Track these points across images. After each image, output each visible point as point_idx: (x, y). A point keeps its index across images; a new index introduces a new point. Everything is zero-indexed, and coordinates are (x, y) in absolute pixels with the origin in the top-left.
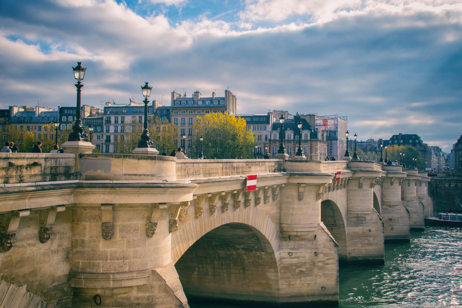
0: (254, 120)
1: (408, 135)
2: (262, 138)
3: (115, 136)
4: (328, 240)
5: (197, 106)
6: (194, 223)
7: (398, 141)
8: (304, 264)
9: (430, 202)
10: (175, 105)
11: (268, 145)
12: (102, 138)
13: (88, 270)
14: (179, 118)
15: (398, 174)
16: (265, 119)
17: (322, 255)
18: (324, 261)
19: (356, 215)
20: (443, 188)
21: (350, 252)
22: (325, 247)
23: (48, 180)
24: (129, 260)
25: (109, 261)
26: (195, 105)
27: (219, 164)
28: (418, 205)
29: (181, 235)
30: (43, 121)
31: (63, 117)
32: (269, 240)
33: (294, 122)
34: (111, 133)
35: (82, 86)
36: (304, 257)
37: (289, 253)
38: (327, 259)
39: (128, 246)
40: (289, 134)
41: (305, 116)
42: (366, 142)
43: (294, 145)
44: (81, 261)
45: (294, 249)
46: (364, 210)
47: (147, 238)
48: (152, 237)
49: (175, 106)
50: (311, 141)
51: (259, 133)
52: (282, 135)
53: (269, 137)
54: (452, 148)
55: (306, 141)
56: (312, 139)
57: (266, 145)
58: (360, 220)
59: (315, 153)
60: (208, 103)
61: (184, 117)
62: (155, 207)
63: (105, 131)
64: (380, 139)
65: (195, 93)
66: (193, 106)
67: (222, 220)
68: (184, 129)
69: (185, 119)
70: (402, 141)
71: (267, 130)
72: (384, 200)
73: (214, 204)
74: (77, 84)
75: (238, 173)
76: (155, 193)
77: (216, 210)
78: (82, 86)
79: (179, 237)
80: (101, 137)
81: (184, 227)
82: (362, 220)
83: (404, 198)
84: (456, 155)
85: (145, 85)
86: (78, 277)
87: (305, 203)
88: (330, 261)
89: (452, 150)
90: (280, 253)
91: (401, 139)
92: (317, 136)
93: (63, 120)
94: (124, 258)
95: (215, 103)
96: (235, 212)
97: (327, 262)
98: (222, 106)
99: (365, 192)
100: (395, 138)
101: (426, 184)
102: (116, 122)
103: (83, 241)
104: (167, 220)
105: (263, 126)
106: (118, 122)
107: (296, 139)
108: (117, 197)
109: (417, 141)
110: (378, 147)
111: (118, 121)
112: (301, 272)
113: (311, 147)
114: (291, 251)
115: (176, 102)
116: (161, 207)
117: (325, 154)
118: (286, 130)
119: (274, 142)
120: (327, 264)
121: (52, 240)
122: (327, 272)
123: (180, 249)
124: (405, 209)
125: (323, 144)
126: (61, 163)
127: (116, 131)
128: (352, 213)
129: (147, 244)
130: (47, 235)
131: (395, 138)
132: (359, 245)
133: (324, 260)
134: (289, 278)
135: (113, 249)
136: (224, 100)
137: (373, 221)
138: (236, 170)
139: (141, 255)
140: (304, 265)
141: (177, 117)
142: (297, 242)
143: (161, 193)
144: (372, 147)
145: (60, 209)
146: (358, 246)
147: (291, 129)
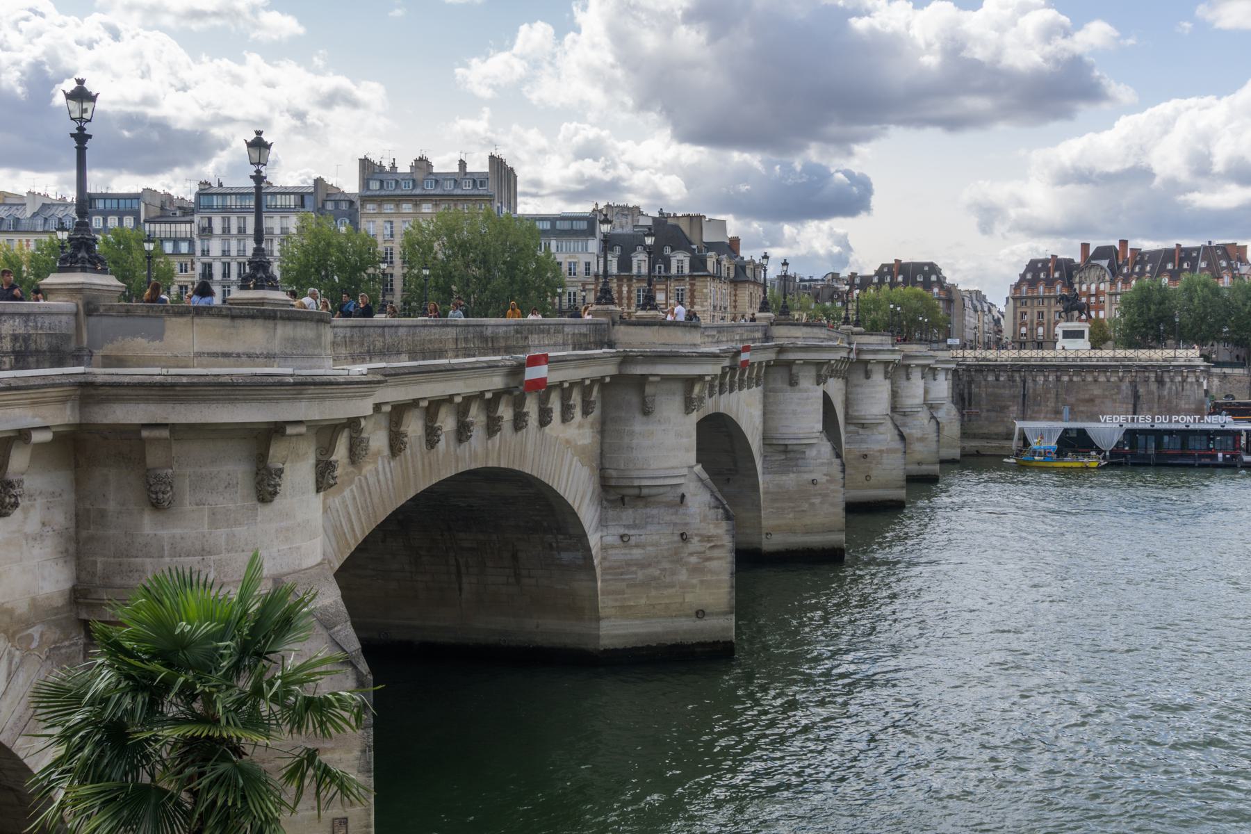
1: (913, 263)
2: (578, 270)
3: (224, 263)
4: (712, 504)
6: (387, 469)
7: (892, 279)
10: (368, 189)
11: (592, 287)
12: (193, 269)
13: (118, 581)
16: (583, 225)
18: (704, 552)
19: (782, 448)
20: (983, 383)
22: (704, 519)
23: (7, 366)
24: (217, 557)
25: (167, 559)
27: (449, 329)
28: (926, 422)
29: (354, 498)
30: (46, 229)
31: (94, 218)
32: (575, 508)
34: (215, 258)
35: (90, 137)
36: (655, 544)
37: (622, 537)
39: (214, 523)
42: (823, 280)
44: (100, 560)
45: (634, 526)
46: (801, 436)
47: (259, 505)
48: (271, 501)
49: (368, 193)
50: (692, 277)
51: (570, 257)
53: (593, 268)
54: (1008, 294)
55: (680, 278)
56: (695, 274)
57: (587, 287)
58: (791, 459)
59: (702, 306)
60: (449, 187)
62: (276, 432)
63: (198, 253)
65: (416, 161)
67: (457, 461)
68: (392, 249)
69: (394, 225)
70: (900, 278)
71: (590, 251)
72: (850, 412)
73: (436, 425)
74: (76, 132)
75: (496, 351)
76: (275, 399)
77: (442, 438)
78: (90, 137)
79: (349, 502)
80: (189, 266)
81: (362, 478)
82: (798, 459)
83: (896, 408)
84: (1015, 308)
85: (255, 136)
86: (95, 596)
88: (716, 553)
89: (1007, 298)
90: (601, 537)
91: (899, 274)
92: (706, 266)
93: (94, 225)
94: (204, 552)
95: (467, 189)
96: (489, 442)
97: (709, 554)
99: (805, 395)
100: (886, 270)
101: (947, 374)
102: (226, 230)
103: (103, 514)
104: (312, 461)
106: (229, 231)
108: (180, 408)
109: (934, 278)
111: (229, 227)
113: (692, 291)
114: (626, 532)
116: (290, 430)
117: (725, 308)
118: (635, 250)
121: (26, 511)
123: (353, 530)
124: (896, 432)
125: (720, 285)
126: (39, 325)
127: (225, 253)
128: (775, 442)
129: (259, 519)
130: (10, 497)
131: (886, 270)
133: (703, 549)
134: (623, 592)
135: (178, 531)
138: (490, 345)
139: (247, 544)
142: (640, 511)
143: (289, 399)
144: (834, 292)
145: (37, 437)
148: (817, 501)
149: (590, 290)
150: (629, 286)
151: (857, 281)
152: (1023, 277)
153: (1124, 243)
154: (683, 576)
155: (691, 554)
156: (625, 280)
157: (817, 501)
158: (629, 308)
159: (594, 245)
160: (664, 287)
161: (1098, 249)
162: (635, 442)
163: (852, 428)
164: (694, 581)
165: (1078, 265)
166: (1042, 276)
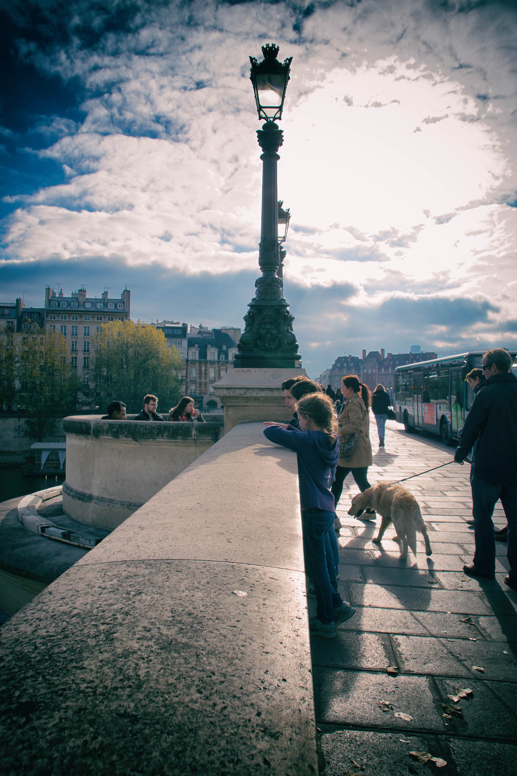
5: (84, 309)
14: (58, 326)
16: (180, 332)
26: (82, 309)
33: (214, 337)
40: (212, 354)
43: (219, 367)
49: (51, 309)
52: (203, 355)
60: (99, 306)
61: (65, 325)
65: (80, 290)
66: (79, 309)
69: (67, 328)
95: (111, 307)
98: (121, 311)
105: (178, 340)
107: (221, 359)
115: (52, 302)
119: (191, 363)
136: (124, 303)
147: (212, 346)
149: (184, 368)
150: (206, 367)
152: (334, 366)
153: (383, 350)
156: (203, 363)
158: (206, 379)
159: (185, 343)
160: (225, 368)
161: (370, 352)
165: (361, 360)
166: (345, 365)
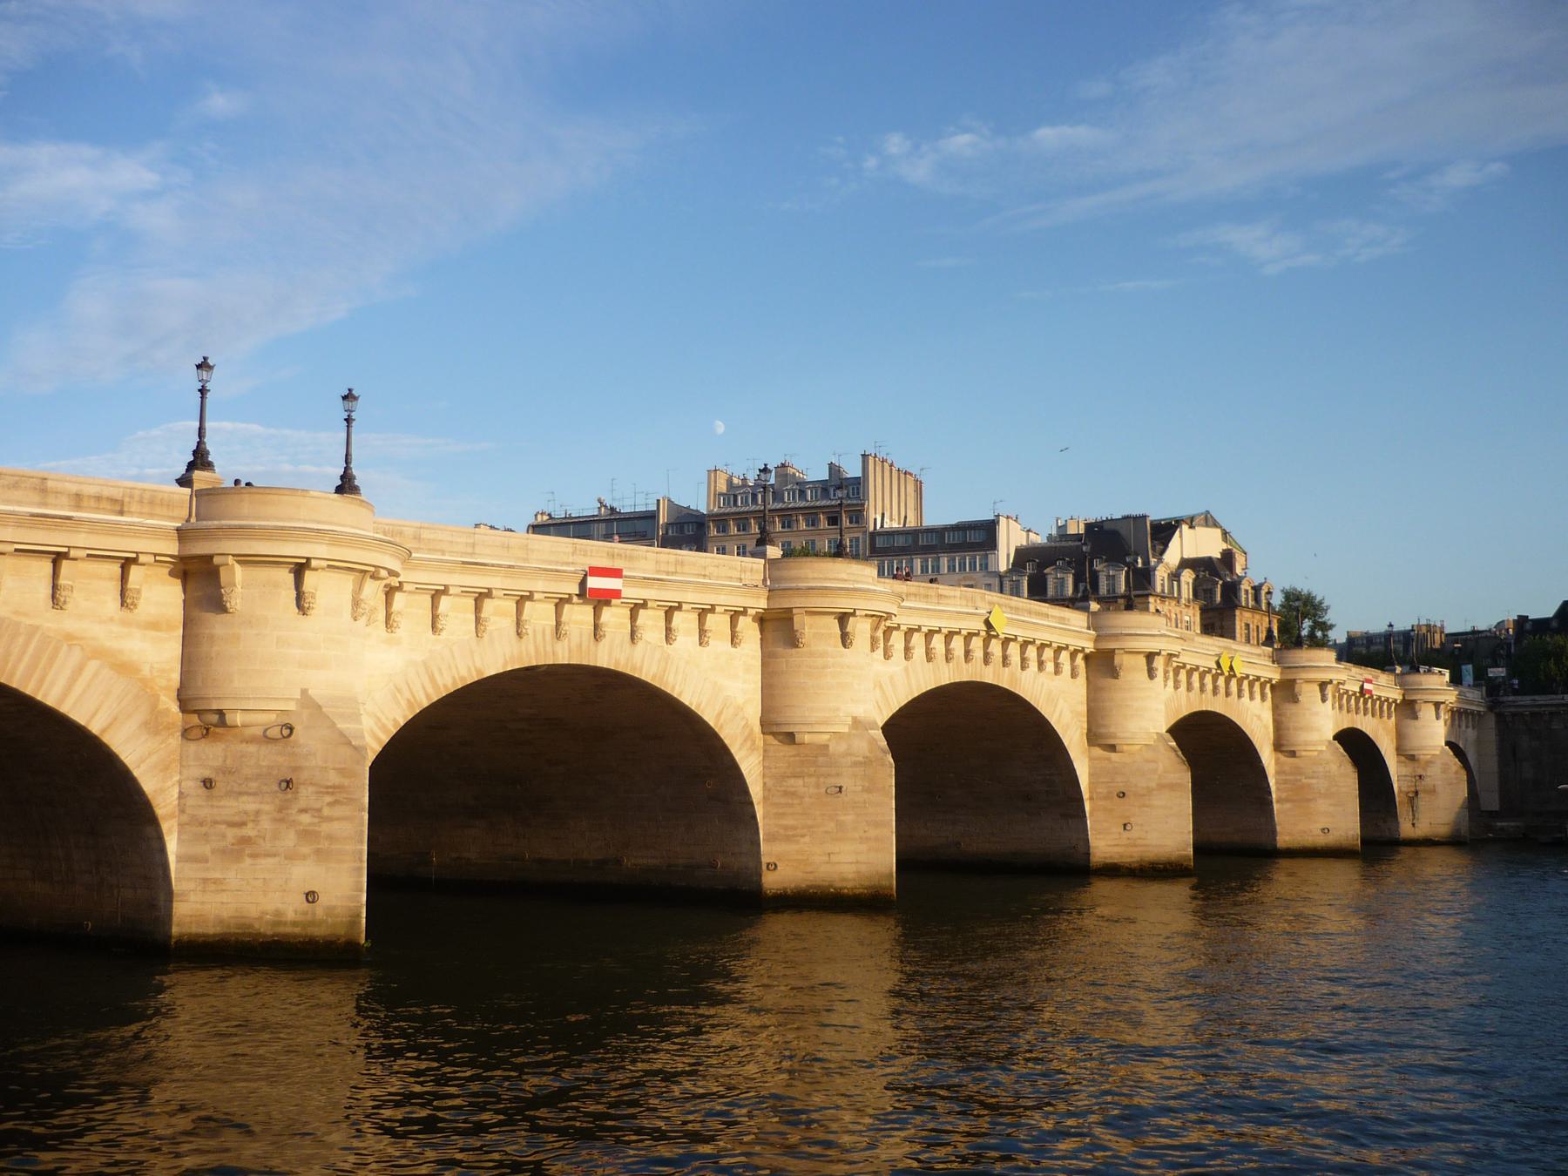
0: (949, 539)
8: (252, 818)
9: (1456, 773)
15: (1113, 638)
17: (311, 789)
18: (319, 810)
21: (771, 861)
38: (330, 804)
41: (1116, 519)
64: (1518, 616)
71: (990, 570)
83: (1282, 745)
87: (250, 622)
90: (180, 783)
97: (326, 812)
110: (1515, 644)
112: (246, 841)
120: (330, 819)
122: (324, 845)
125: (1178, 609)
132: (803, 836)
133: (317, 806)
137: (854, 759)
140: (253, 821)
141: (723, 544)
146: (802, 840)
148: (848, 818)
151: (1528, 626)
154: (289, 839)
155: (304, 811)
157: (848, 818)
162: (216, 648)
163: (1098, 751)
164: (306, 850)
